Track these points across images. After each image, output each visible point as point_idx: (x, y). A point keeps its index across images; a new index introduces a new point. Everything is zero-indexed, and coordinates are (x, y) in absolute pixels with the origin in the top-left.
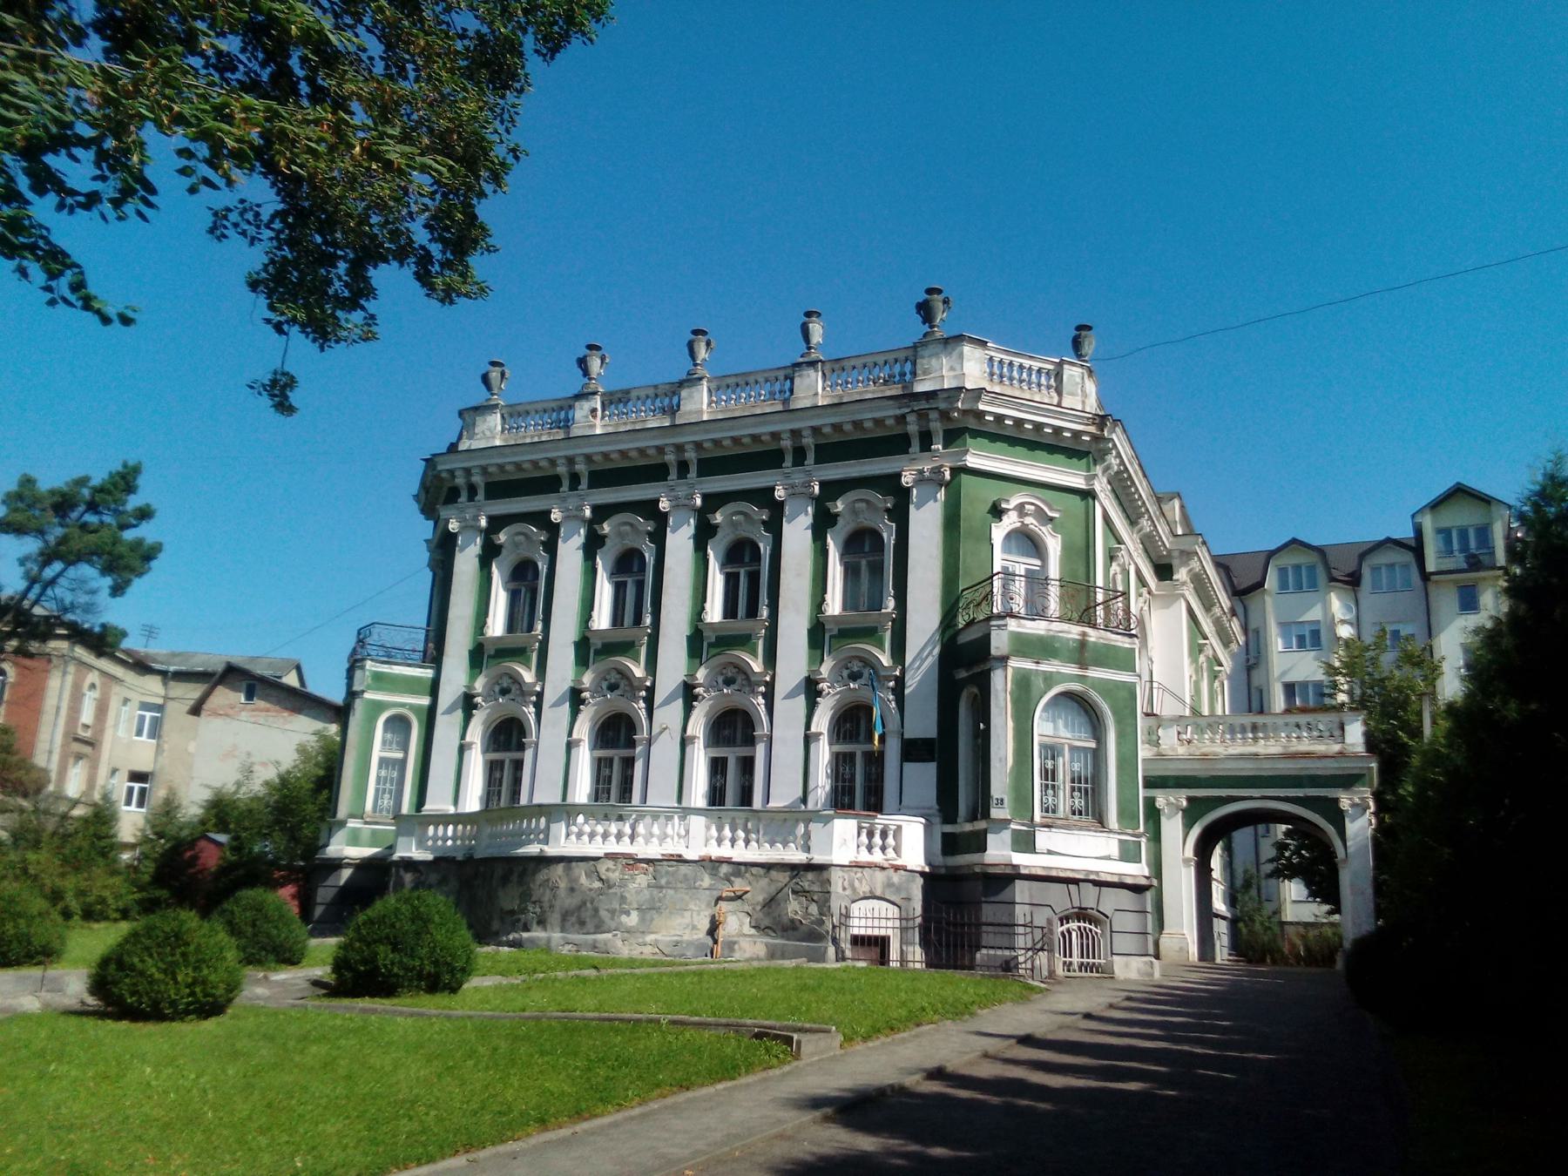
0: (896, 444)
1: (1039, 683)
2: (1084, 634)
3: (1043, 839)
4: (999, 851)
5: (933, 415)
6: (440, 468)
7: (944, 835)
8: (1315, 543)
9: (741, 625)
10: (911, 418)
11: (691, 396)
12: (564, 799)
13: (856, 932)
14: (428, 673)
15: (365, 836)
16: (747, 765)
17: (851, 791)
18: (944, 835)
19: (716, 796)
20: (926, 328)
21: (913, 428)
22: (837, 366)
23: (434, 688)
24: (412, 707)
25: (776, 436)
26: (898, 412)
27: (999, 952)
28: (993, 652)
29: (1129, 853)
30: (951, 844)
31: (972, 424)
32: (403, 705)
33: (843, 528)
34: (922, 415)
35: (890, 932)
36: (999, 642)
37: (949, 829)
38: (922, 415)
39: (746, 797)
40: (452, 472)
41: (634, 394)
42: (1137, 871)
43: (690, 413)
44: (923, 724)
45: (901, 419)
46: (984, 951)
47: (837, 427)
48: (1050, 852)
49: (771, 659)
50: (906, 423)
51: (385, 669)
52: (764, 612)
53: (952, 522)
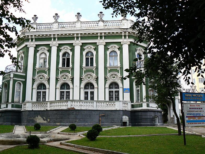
0: (120, 37)
3: (151, 105)
4: (144, 107)
5: (127, 33)
7: (132, 105)
10: (123, 33)
12: (55, 99)
13: (124, 121)
16: (92, 93)
17: (113, 98)
18: (132, 105)
19: (86, 98)
21: (123, 34)
24: (21, 81)
25: (97, 33)
30: (133, 106)
31: (133, 34)
32: (20, 81)
33: (110, 50)
34: (125, 32)
37: (132, 104)
38: (125, 32)
39: (92, 98)
40: (28, 36)
43: (78, 28)
45: (121, 33)
47: (109, 33)
48: (151, 107)
49: (97, 74)
52: (71, 66)
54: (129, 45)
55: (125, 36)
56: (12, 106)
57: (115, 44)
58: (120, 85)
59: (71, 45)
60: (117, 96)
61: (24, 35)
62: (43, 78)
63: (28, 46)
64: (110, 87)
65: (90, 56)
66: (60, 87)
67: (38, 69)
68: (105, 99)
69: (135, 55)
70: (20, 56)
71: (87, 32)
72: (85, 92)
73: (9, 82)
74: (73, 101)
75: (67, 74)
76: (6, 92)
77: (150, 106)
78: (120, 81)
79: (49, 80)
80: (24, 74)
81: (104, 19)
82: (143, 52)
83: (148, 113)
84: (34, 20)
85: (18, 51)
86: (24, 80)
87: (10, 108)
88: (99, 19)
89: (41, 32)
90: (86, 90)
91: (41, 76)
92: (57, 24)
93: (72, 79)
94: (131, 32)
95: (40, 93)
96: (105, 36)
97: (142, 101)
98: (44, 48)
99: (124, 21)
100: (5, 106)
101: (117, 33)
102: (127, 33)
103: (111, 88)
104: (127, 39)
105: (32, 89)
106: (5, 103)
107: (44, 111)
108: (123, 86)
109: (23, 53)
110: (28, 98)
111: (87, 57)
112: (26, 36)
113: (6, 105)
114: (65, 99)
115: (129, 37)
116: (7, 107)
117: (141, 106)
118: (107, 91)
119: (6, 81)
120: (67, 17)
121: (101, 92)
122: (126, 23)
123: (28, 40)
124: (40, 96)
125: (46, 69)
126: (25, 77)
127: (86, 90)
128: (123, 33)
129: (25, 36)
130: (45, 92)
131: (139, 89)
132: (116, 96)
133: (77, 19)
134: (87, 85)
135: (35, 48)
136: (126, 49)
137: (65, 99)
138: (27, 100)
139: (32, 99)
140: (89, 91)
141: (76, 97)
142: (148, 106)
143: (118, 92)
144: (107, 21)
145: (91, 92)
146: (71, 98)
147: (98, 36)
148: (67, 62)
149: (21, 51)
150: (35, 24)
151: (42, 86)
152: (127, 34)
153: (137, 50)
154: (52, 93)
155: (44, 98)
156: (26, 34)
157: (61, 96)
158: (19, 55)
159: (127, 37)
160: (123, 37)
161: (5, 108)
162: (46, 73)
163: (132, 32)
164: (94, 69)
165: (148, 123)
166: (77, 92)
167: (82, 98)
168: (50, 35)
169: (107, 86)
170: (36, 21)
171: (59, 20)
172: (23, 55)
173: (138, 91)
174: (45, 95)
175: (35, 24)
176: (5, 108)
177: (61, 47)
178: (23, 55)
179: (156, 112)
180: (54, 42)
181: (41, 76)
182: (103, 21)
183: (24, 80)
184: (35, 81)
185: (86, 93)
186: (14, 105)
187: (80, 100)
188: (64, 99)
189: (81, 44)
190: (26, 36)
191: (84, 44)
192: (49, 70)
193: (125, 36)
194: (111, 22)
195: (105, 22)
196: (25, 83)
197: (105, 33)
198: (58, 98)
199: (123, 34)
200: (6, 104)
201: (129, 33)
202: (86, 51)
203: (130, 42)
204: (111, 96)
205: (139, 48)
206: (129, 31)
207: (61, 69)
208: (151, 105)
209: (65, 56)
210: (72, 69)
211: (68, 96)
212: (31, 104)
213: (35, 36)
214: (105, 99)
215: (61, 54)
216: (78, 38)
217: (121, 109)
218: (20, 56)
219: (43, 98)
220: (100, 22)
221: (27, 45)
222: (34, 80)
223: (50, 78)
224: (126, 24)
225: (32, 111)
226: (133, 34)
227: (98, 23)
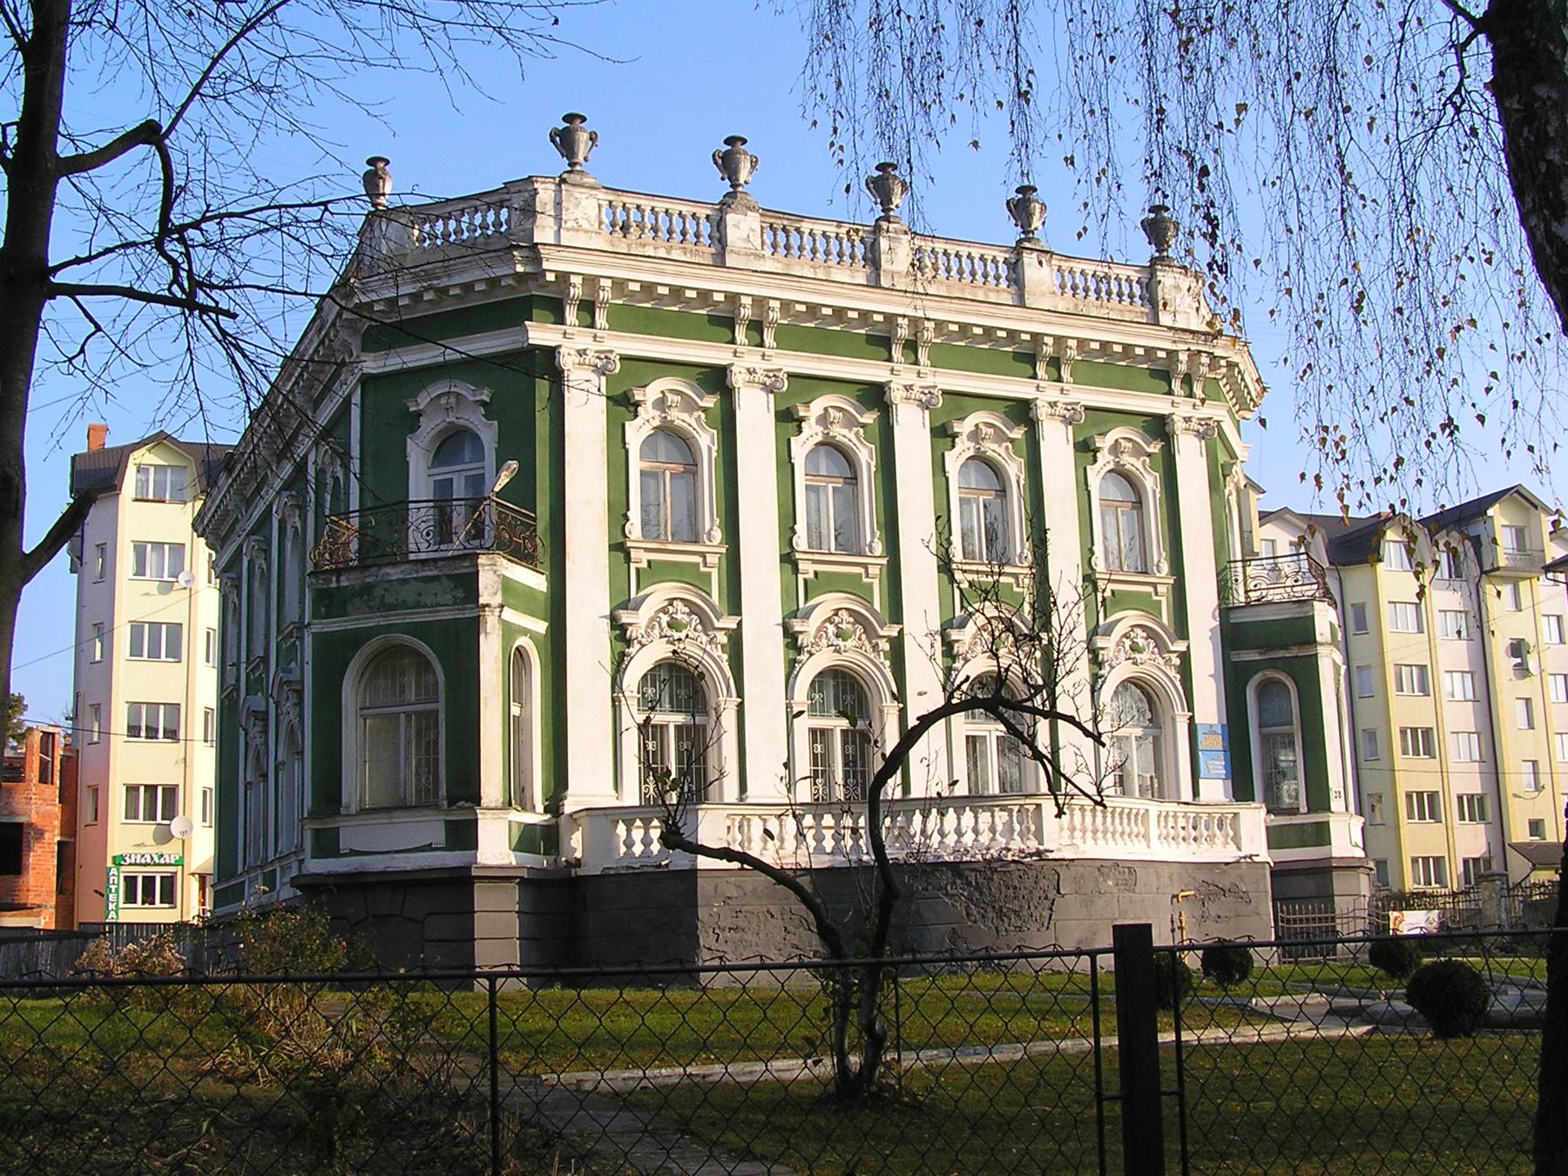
6: (545, 265)
10: (1183, 357)
23: (556, 608)
26: (1174, 347)
28: (1319, 638)
40: (563, 277)
59: (875, 396)
70: (429, 427)
97: (1319, 798)
100: (431, 828)
119: (418, 630)
128: (1183, 357)
161: (429, 848)
176: (429, 848)
190: (550, 277)
200: (447, 822)
218: (429, 427)
221: (551, 352)
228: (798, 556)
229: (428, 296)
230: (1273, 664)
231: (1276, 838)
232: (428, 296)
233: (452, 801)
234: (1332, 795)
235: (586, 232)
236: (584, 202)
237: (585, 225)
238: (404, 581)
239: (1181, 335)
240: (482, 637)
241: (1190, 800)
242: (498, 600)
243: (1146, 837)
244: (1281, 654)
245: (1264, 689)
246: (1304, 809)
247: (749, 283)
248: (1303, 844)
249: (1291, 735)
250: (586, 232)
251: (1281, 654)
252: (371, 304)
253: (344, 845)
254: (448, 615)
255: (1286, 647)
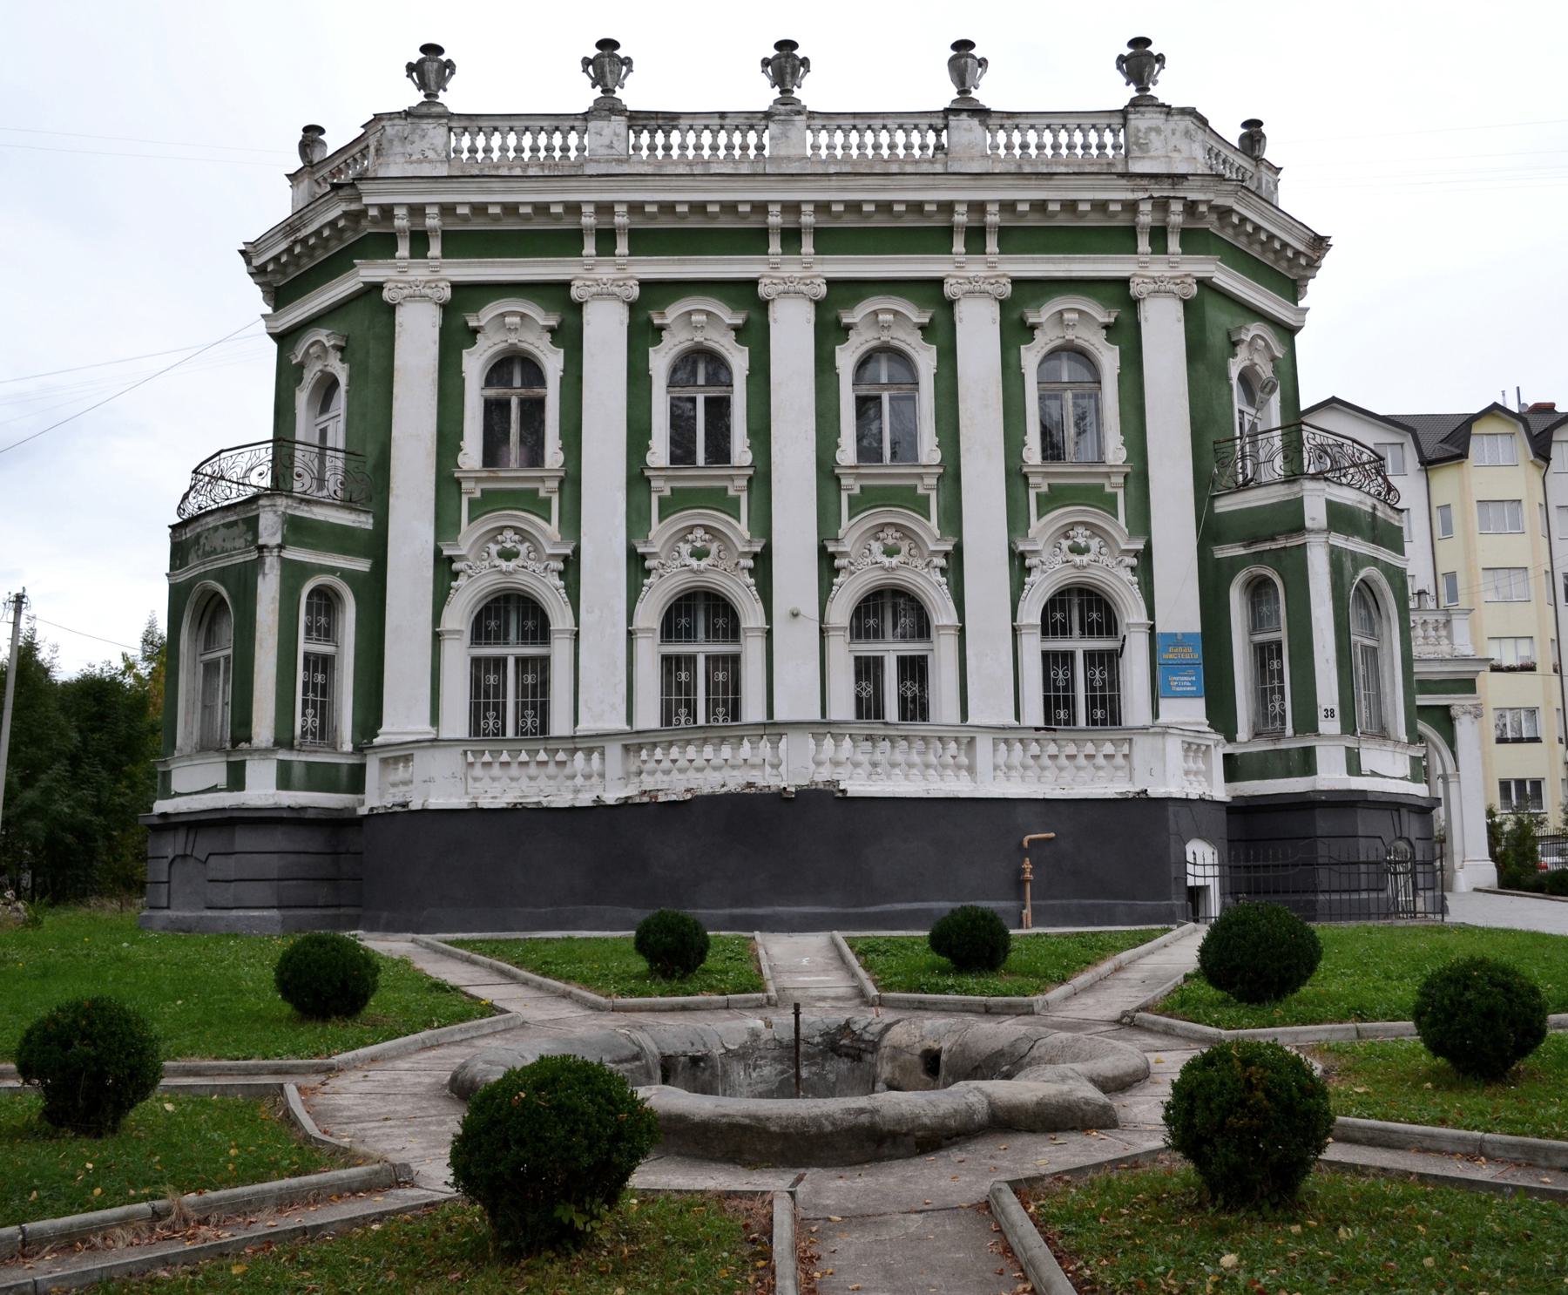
0: (1121, 238)
1: (1348, 564)
2: (1374, 508)
3: (1372, 757)
4: (1331, 775)
5: (1177, 207)
6: (366, 200)
7: (1227, 757)
8: (1381, 413)
9: (701, 473)
10: (1146, 207)
11: (785, 135)
13: (1191, 882)
14: (365, 522)
15: (298, 773)
16: (914, 669)
17: (1069, 703)
19: (869, 707)
20: (1131, 92)
21: (1146, 217)
22: (1007, 123)
24: (346, 575)
25: (947, 207)
26: (1130, 196)
27: (1335, 897)
28: (1308, 524)
29: (1420, 771)
31: (1211, 223)
32: (332, 570)
34: (1162, 205)
35: (1209, 881)
36: (1315, 514)
37: (1229, 749)
38: (1162, 205)
39: (915, 708)
40: (387, 211)
41: (684, 123)
42: (1420, 790)
43: (788, 158)
44: (1180, 610)
45: (1132, 207)
46: (1321, 897)
47: (1040, 206)
48: (1374, 774)
50: (424, 215)
51: (304, 512)
53: (1196, 349)
54: (1189, 306)
55: (1159, 237)
56: (285, 780)
57: (1088, 295)
58: (1131, 612)
59: (744, 293)
60: (1102, 689)
61: (354, 207)
62: (523, 548)
63: (386, 295)
64: (1050, 627)
65: (701, 380)
66: (657, 625)
67: (478, 480)
68: (1017, 717)
69: (1228, 379)
71: (868, 194)
72: (857, 659)
73: (244, 581)
74: (772, 728)
75: (718, 519)
76: (211, 668)
77: (1365, 767)
78: (1128, 576)
79: (571, 568)
80: (365, 522)
81: (987, 94)
82: (1274, 359)
83: (1365, 823)
84: (422, 85)
85: (285, 339)
86: (363, 565)
87: (261, 789)
88: (944, 94)
89: (496, 185)
90: (868, 649)
91: (509, 534)
92: (619, 123)
93: (755, 556)
94: (1208, 202)
95: (496, 672)
96: (1004, 233)
97: (1307, 721)
98: (523, 316)
99: (1139, 122)
100: (216, 772)
101: (1101, 206)
102: (1177, 207)
103: (1055, 633)
104: (1143, 258)
105: (437, 637)
106: (206, 747)
107: (572, 809)
108: (1151, 614)
109: (341, 349)
110: (403, 717)
111: (865, 391)
112: (373, 212)
113: (224, 766)
114: (701, 720)
115: (1194, 240)
116: (236, 780)
117: (1306, 763)
118: (1033, 647)
119: (221, 575)
120: (697, 69)
121: (990, 657)
122: (1158, 130)
123: (383, 245)
124: (500, 689)
125: (542, 479)
126: (376, 545)
127: (868, 649)
128: (1146, 207)
129: (362, 213)
130: (544, 663)
131: (1283, 635)
132: (1093, 689)
133: (776, 93)
134: (867, 607)
135: (447, 309)
136: (1163, 331)
137: (701, 720)
138: (394, 729)
139: (435, 719)
140: (890, 651)
141: (796, 702)
142: (1354, 765)
143: (1107, 661)
144: (1011, 115)
145: (903, 662)
146: (753, 710)
147: (948, 232)
148: (704, 430)
149: (322, 335)
150: (440, 116)
151: (511, 614)
152: (1176, 218)
153: (1235, 344)
154: (605, 666)
155: (534, 708)
156: (373, 198)
157: (669, 693)
158: (301, 366)
159: (1174, 244)
160: (1143, 244)
162: (540, 507)
163: (1213, 208)
164: (737, 488)
165: (1364, 895)
166: (797, 662)
167: (843, 706)
168: (574, 209)
169: (1031, 613)
170: (441, 93)
171: (635, 94)
172: (341, 372)
173: (1265, 654)
174: (544, 686)
175: (440, 116)
177: (661, 305)
178: (341, 372)
179: (1404, 811)
180: (417, 266)
181: (509, 534)
182: (982, 113)
183: (363, 565)
184: (455, 575)
185: (867, 670)
186: (298, 773)
187: (823, 727)
188: (693, 713)
189: (824, 290)
190: (373, 212)
191: (656, 292)
192: (567, 488)
193: (1159, 237)
194: (852, 122)
195: (992, 122)
196: (372, 592)
197: (1008, 207)
198: (649, 715)
199: (1146, 217)
200: (229, 763)
201: (1191, 207)
202: (862, 339)
203: (1204, 283)
204: (1057, 689)
205: (1256, 328)
206: (1192, 196)
207: (668, 478)
208: (1372, 757)
209: (692, 381)
210: (750, 480)
211: (728, 699)
212: (460, 758)
213: (447, 210)
214: (1017, 717)
215: (474, 364)
216: (791, 238)
217: (1175, 791)
218: (310, 376)
219: (521, 708)
220: (964, 116)
221: (378, 287)
222: (445, 570)
223: (577, 551)
224: (1156, 141)
225: (476, 813)
226: (1213, 217)
227: (939, 123)
228: (647, 473)
229: (297, 250)
230: (1258, 558)
231: (1234, 768)
232: (297, 250)
233: (235, 742)
234: (1321, 714)
235: (431, 162)
236: (431, 133)
237: (431, 154)
238: (216, 528)
239: (1138, 181)
240: (260, 579)
241: (1041, 723)
242: (277, 540)
243: (971, 769)
244: (1267, 546)
245: (1258, 590)
246: (1289, 731)
247: (588, 191)
248: (1289, 774)
249: (1279, 644)
250: (431, 162)
251: (1267, 546)
252: (265, 264)
253: (177, 784)
254: (240, 559)
255: (1273, 539)
